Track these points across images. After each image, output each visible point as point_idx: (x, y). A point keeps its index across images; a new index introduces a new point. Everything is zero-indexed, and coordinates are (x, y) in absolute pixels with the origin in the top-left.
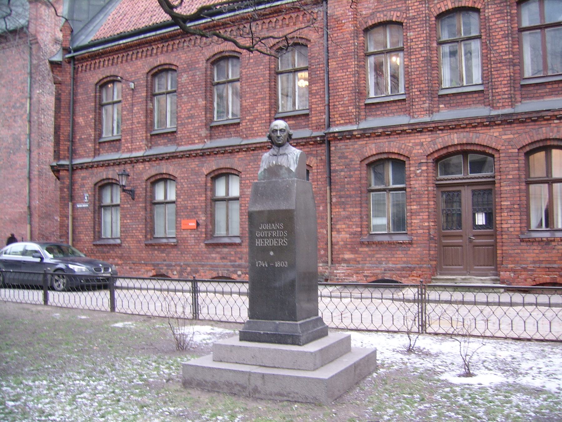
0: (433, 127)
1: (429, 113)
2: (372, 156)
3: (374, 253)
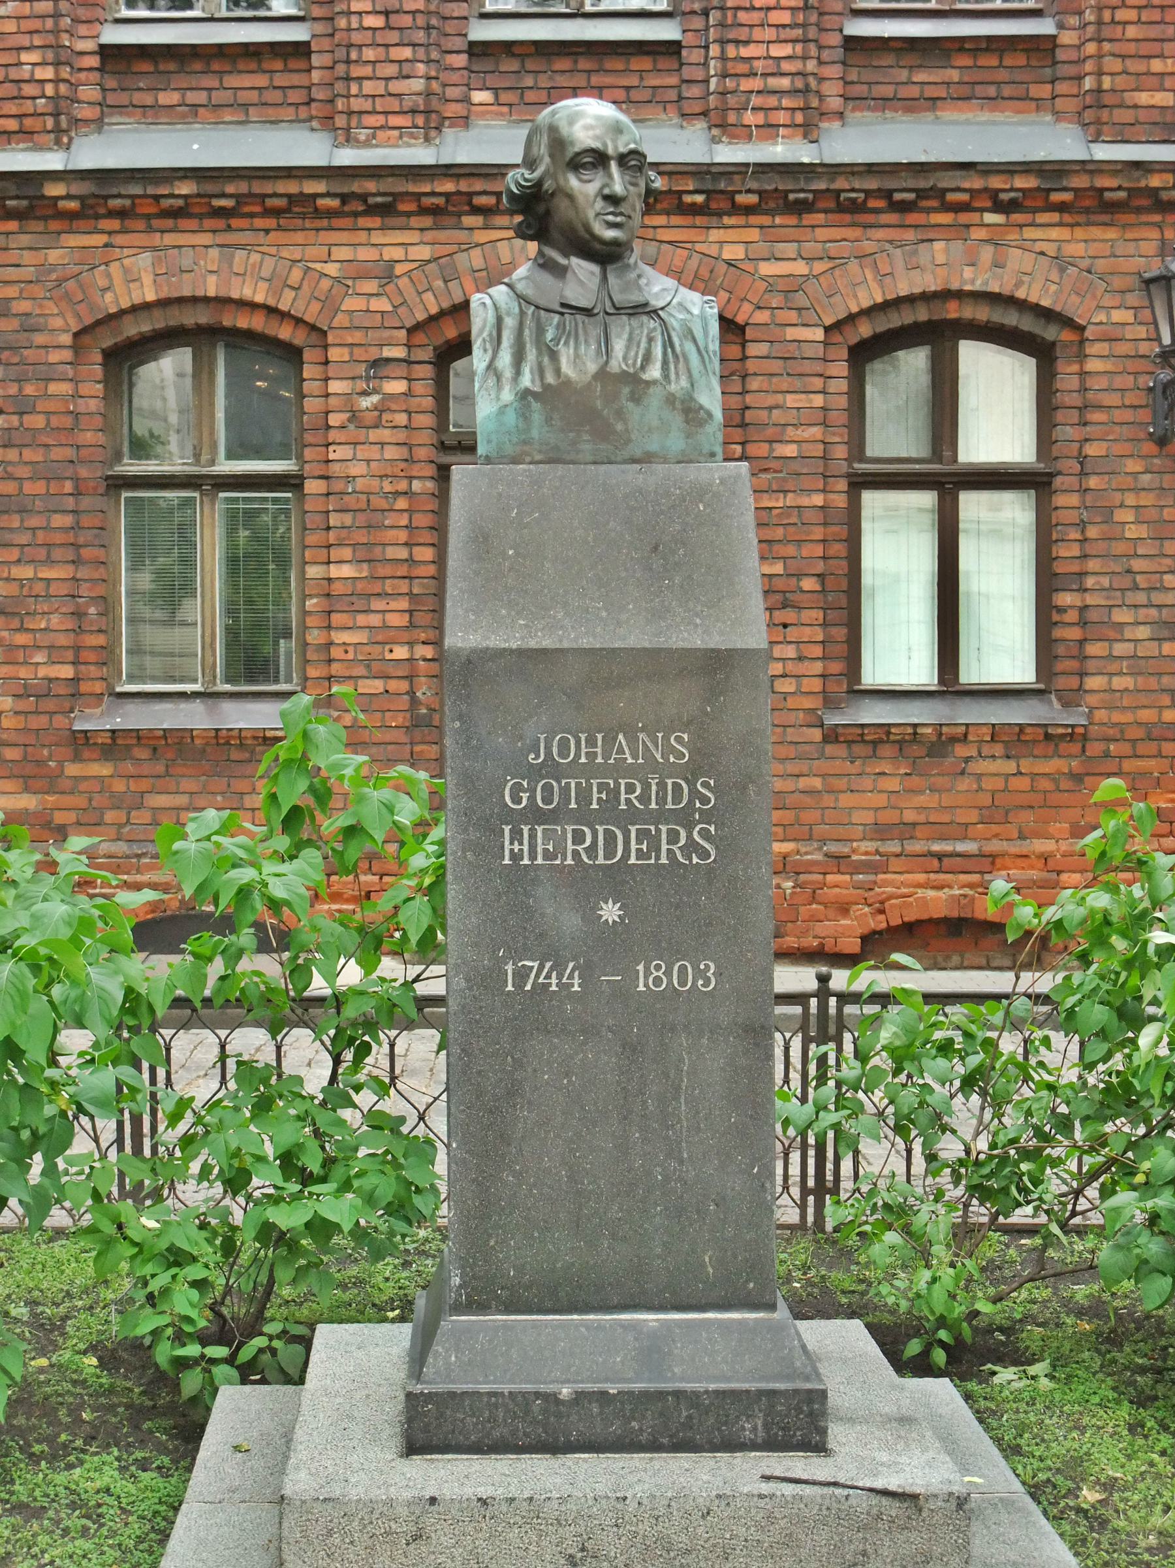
0: (447, 195)
1: (427, 127)
2: (134, 309)
3: (144, 785)
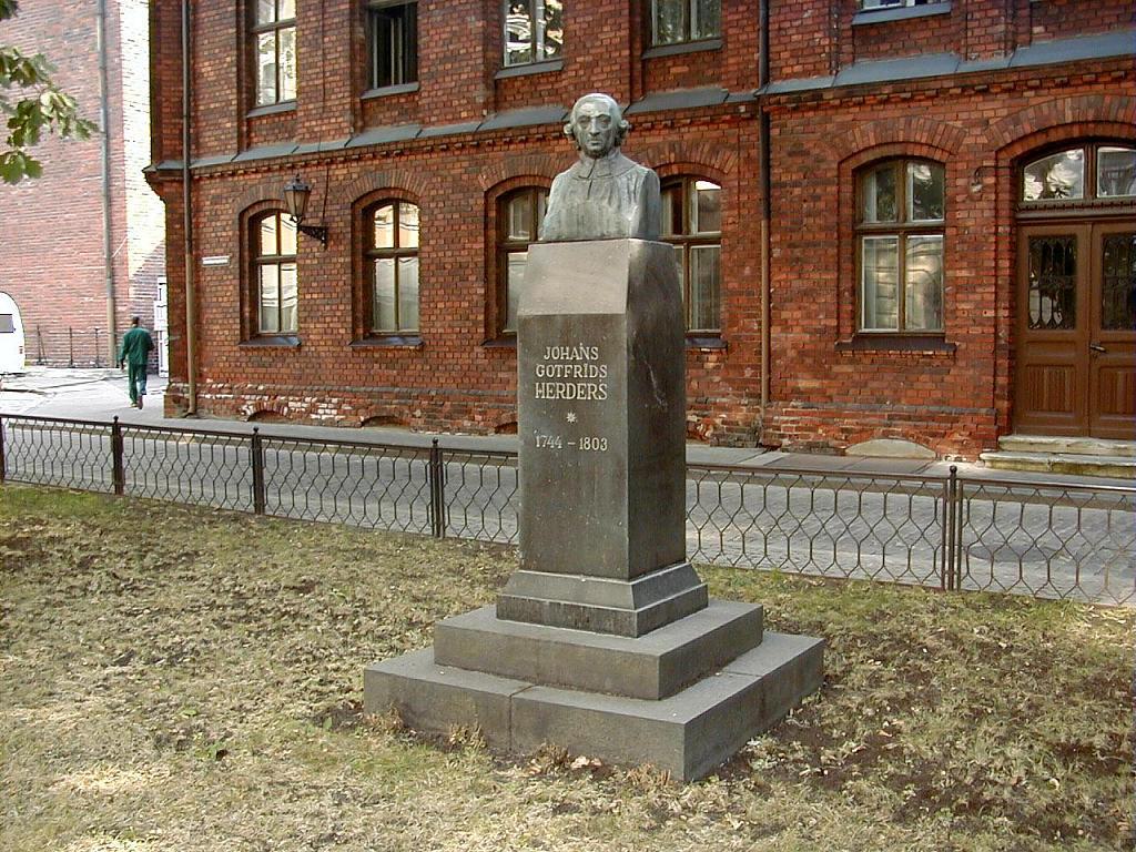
2: (866, 149)
